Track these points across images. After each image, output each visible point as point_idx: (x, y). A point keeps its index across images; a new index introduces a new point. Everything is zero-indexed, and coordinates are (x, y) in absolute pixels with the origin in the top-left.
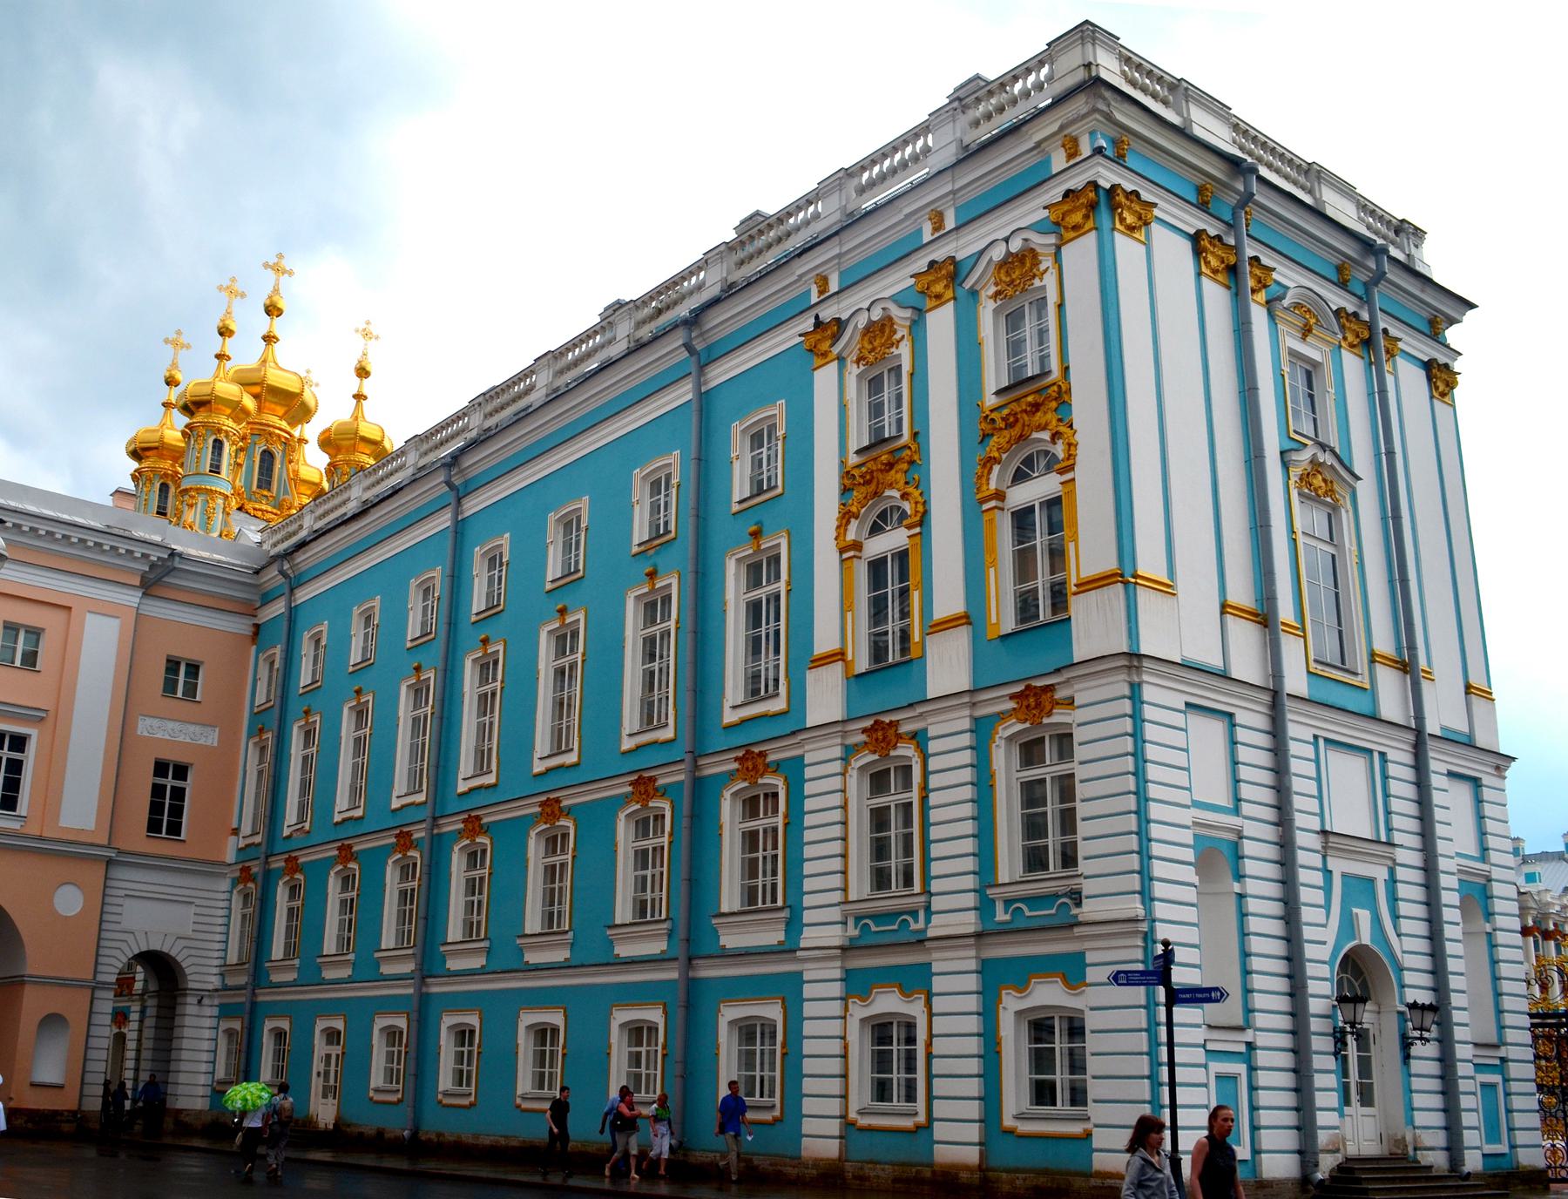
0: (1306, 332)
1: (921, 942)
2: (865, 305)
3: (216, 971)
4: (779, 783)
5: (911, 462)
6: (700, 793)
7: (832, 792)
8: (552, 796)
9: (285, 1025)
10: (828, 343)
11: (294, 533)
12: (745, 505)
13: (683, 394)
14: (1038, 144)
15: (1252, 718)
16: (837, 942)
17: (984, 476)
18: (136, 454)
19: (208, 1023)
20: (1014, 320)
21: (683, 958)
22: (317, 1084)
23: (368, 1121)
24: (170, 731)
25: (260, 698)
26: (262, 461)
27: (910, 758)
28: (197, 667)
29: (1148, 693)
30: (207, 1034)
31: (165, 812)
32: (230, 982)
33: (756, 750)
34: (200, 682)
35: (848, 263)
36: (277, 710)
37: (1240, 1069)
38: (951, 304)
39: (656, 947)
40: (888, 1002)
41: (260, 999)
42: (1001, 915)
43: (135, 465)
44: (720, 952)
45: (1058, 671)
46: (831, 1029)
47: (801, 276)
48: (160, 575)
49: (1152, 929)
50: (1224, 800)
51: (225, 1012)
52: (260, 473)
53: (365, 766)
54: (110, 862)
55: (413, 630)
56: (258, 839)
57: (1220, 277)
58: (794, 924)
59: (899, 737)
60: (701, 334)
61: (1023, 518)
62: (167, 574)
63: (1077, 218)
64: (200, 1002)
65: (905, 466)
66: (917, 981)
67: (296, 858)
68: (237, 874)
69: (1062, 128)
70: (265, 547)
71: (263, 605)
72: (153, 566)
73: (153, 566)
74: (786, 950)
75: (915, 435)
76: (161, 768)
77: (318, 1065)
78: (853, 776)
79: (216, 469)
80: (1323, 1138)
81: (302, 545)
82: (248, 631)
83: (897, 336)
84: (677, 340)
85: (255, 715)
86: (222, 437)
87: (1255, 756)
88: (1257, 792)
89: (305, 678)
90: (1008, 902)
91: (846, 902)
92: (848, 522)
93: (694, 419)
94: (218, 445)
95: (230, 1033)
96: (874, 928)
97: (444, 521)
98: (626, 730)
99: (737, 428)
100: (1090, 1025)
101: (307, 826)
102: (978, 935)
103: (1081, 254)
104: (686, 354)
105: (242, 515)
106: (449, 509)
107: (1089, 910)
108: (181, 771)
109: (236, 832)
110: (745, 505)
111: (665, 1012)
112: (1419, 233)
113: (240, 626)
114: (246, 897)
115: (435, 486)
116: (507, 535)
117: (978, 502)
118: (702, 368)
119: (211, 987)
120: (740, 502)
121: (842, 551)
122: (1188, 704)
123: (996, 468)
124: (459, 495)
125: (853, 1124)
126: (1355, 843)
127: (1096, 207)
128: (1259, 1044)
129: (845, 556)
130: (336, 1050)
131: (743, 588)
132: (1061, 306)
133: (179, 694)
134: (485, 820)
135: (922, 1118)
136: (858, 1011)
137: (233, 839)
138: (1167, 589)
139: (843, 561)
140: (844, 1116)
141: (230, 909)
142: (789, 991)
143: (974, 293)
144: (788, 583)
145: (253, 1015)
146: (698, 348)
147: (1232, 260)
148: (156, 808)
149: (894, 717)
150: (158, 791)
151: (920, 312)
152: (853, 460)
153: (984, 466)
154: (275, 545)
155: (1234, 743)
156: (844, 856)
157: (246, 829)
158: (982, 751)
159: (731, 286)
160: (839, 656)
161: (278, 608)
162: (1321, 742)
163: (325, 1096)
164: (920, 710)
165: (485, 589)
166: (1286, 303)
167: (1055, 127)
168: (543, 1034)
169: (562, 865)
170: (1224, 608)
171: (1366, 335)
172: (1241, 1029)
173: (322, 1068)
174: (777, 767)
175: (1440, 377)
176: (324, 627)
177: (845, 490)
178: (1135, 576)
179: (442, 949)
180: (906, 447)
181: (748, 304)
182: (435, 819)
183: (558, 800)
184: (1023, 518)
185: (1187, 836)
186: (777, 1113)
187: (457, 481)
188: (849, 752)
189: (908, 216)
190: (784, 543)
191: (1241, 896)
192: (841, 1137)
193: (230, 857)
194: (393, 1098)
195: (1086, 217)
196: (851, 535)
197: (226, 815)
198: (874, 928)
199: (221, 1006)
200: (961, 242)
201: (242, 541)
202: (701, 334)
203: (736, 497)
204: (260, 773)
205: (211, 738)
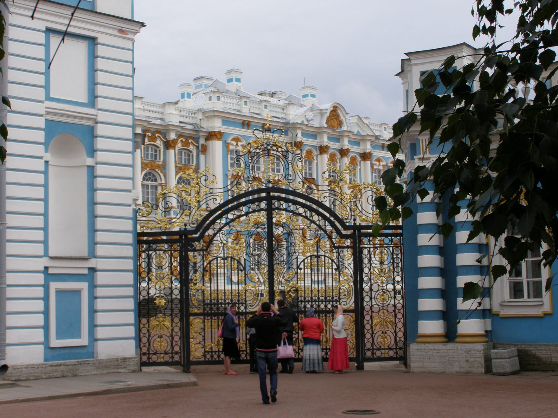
37: (84, 286)
50: (83, 98)
185: (41, 122)
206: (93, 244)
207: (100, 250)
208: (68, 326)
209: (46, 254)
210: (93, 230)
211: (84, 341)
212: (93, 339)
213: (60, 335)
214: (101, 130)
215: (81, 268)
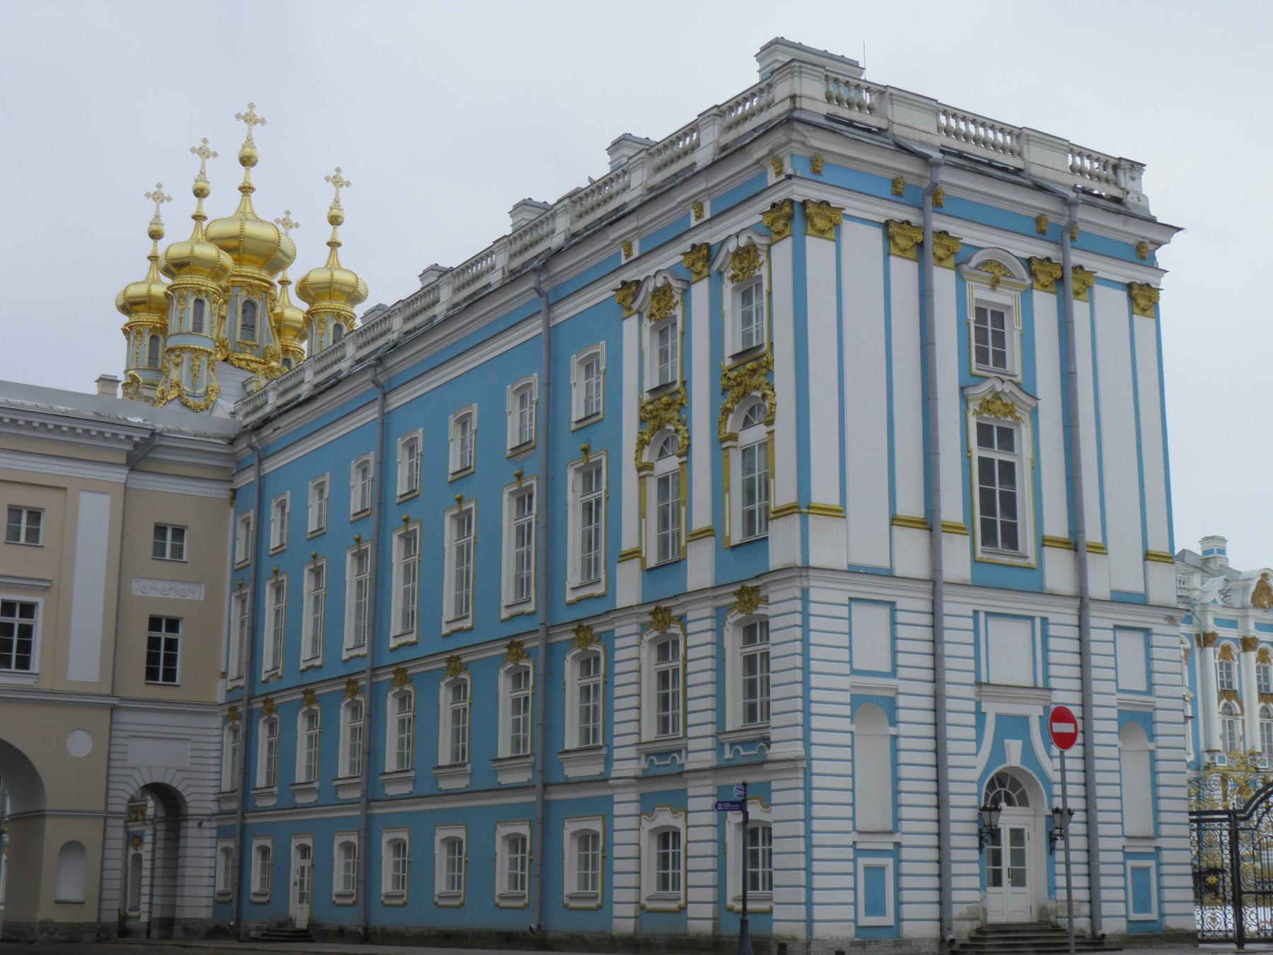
0: (995, 284)
1: (680, 774)
2: (652, 273)
3: (212, 797)
4: (599, 649)
5: (682, 405)
6: (551, 654)
7: (633, 656)
8: (455, 654)
9: (268, 843)
10: (631, 299)
11: (261, 407)
12: (580, 425)
13: (535, 328)
14: (758, 162)
15: (914, 604)
16: (632, 774)
17: (722, 423)
19: (208, 843)
20: (746, 297)
21: (539, 786)
22: (294, 892)
23: (332, 920)
24: (160, 590)
25: (240, 557)
27: (677, 635)
29: (814, 595)
30: (208, 852)
31: (161, 661)
32: (227, 806)
33: (586, 624)
34: (185, 544)
36: (252, 567)
37: (889, 862)
38: (706, 280)
39: (523, 777)
40: (665, 818)
41: (249, 821)
42: (728, 754)
43: (125, 319)
44: (564, 781)
45: (757, 577)
46: (631, 836)
48: (143, 453)
49: (810, 765)
50: (887, 668)
51: (223, 833)
53: (319, 624)
54: (113, 708)
55: (355, 507)
56: (242, 682)
57: (909, 254)
58: (608, 760)
59: (671, 619)
60: (550, 278)
61: (747, 452)
62: (151, 450)
63: (779, 225)
64: (200, 825)
65: (677, 407)
66: (678, 802)
67: (272, 700)
68: (227, 713)
69: (772, 151)
70: (239, 417)
72: (136, 445)
74: (603, 780)
75: (684, 383)
76: (155, 623)
77: (294, 876)
78: (645, 645)
79: (198, 327)
80: (957, 911)
81: (267, 421)
83: (675, 300)
85: (237, 571)
86: (202, 297)
87: (915, 631)
88: (916, 659)
89: (274, 542)
90: (732, 745)
91: (640, 743)
92: (643, 448)
93: (544, 352)
95: (226, 851)
96: (656, 763)
97: (372, 413)
98: (504, 603)
99: (574, 360)
100: (775, 832)
101: (280, 672)
102: (715, 769)
103: (783, 252)
104: (536, 295)
105: (226, 365)
106: (378, 403)
107: (776, 751)
108: (173, 625)
109: (224, 675)
110: (580, 425)
111: (531, 828)
112: (1136, 167)
113: (219, 492)
114: (235, 731)
116: (420, 430)
117: (722, 442)
118: (550, 307)
119: (208, 812)
120: (577, 422)
121: (640, 469)
122: (851, 599)
123: (731, 416)
125: (642, 908)
126: (1012, 690)
127: (793, 217)
128: (904, 843)
129: (642, 474)
130: (307, 863)
132: (770, 293)
133: (168, 556)
134: (410, 672)
135: (682, 902)
136: (647, 825)
137: (221, 683)
138: (838, 513)
139: (640, 478)
140: (638, 903)
141: (222, 743)
142: (604, 808)
143: (720, 273)
144: (607, 493)
145: (243, 836)
146: (546, 289)
147: (920, 238)
148: (152, 658)
149: (668, 604)
150: (153, 643)
151: (689, 283)
152: (646, 397)
153: (723, 413)
154: (247, 415)
155: (894, 623)
156: (639, 708)
157: (233, 673)
158: (719, 631)
160: (635, 554)
161: (249, 477)
162: (982, 616)
163: (301, 901)
164: (681, 600)
166: (973, 263)
167: (765, 151)
168: (453, 844)
169: (465, 710)
170: (894, 520)
171: (1059, 274)
172: (890, 833)
173: (298, 878)
174: (599, 638)
175: (1143, 298)
176: (288, 496)
177: (642, 421)
178: (809, 508)
179: (382, 778)
180: (678, 392)
181: (585, 254)
182: (373, 670)
183: (458, 658)
184: (747, 452)
185: (846, 697)
186: (599, 902)
188: (644, 627)
189: (680, 204)
190: (604, 458)
191: (895, 738)
192: (636, 917)
193: (220, 697)
194: (349, 901)
195: (786, 225)
196: (645, 459)
197: (212, 663)
198: (656, 763)
199: (218, 828)
200: (714, 230)
202: (550, 278)
203: (574, 419)
204: (242, 623)
205: (198, 594)
206: (897, 820)
207: (905, 826)
208: (875, 907)
209: (854, 829)
210: (897, 806)
211: (889, 920)
212: (899, 919)
213: (868, 913)
214: (902, 701)
215: (886, 843)
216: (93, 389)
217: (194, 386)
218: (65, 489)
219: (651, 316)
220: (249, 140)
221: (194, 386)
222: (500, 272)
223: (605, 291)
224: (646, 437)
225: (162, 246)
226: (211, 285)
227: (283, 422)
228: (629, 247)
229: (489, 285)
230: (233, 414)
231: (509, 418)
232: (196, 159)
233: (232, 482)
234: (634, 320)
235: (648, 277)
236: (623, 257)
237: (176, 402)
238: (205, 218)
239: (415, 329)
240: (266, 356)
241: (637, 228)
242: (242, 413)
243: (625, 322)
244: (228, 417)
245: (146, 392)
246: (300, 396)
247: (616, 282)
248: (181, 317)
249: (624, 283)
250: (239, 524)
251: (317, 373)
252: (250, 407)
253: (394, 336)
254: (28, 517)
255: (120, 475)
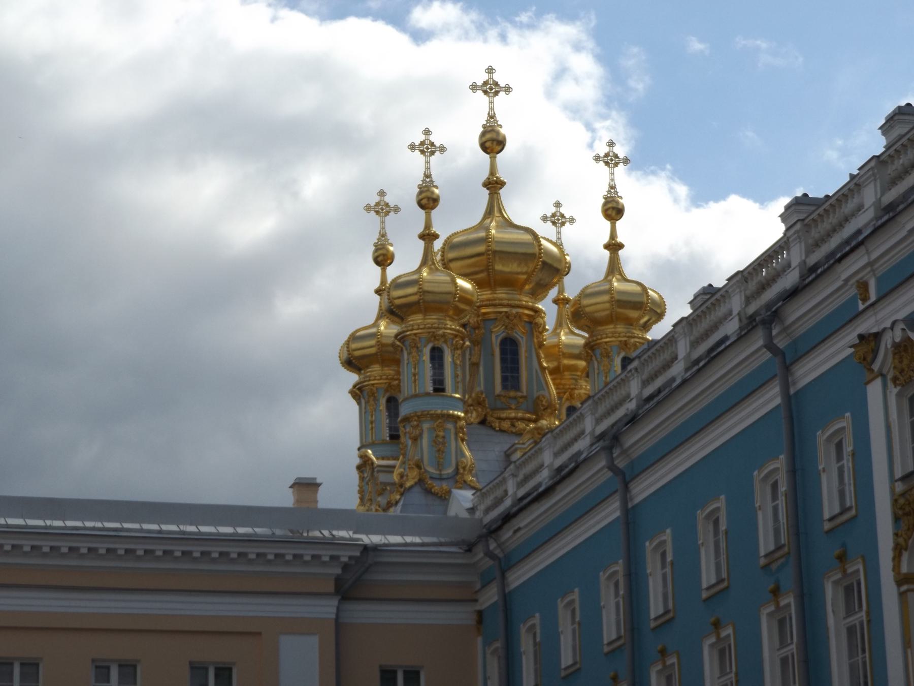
2: (888, 324)
18: (351, 363)
26: (503, 352)
28: (417, 673)
35: (883, 267)
43: (353, 378)
47: (847, 281)
48: (356, 576)
52: (503, 370)
60: (785, 329)
70: (478, 514)
71: (483, 587)
72: (346, 567)
73: (346, 567)
81: (507, 518)
82: (471, 620)
84: (758, 341)
94: (437, 356)
99: (821, 437)
104: (769, 355)
105: (483, 431)
113: (462, 615)
115: (596, 473)
121: (899, 583)
124: (625, 479)
131: (842, 613)
139: (902, 595)
154: (488, 510)
159: (813, 269)
165: (660, 589)
176: (537, 620)
177: (896, 519)
187: (621, 463)
196: (904, 569)
201: (453, 511)
202: (785, 329)
216: (286, 499)
217: (440, 466)
218: (260, 634)
219: (895, 380)
220: (492, 117)
221: (440, 466)
222: (736, 320)
223: (840, 349)
224: (901, 540)
225: (393, 272)
226: (452, 326)
227: (523, 520)
228: (863, 287)
229: (726, 338)
230: (472, 510)
231: (760, 515)
232: (418, 158)
233: (476, 601)
234: (877, 384)
235: (884, 330)
236: (860, 302)
237: (417, 489)
238: (436, 236)
239: (659, 391)
240: (539, 408)
241: (870, 264)
242: (482, 507)
243: (870, 388)
244: (466, 515)
245: (382, 477)
246: (540, 484)
247: (851, 336)
248: (417, 374)
249: (861, 337)
250: (488, 656)
251: (556, 455)
252: (489, 501)
253: (632, 406)
254: (217, 676)
255: (327, 609)
